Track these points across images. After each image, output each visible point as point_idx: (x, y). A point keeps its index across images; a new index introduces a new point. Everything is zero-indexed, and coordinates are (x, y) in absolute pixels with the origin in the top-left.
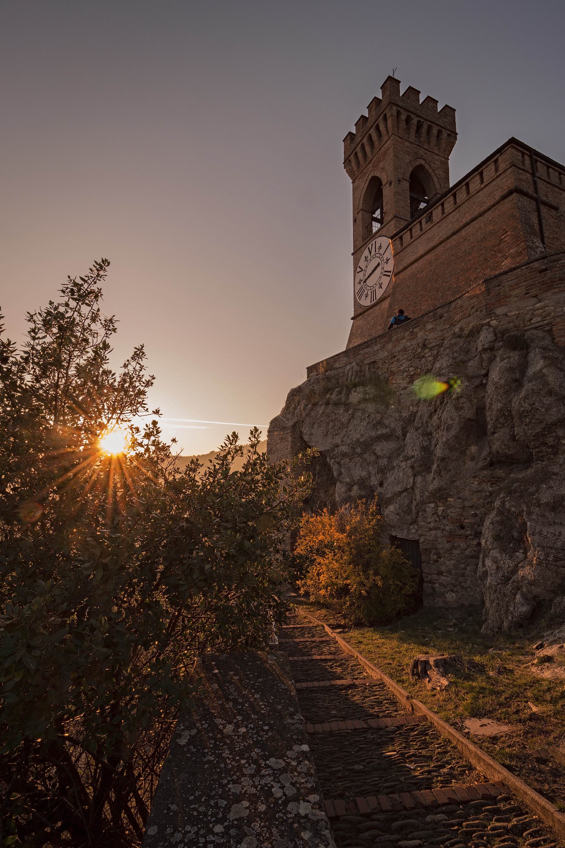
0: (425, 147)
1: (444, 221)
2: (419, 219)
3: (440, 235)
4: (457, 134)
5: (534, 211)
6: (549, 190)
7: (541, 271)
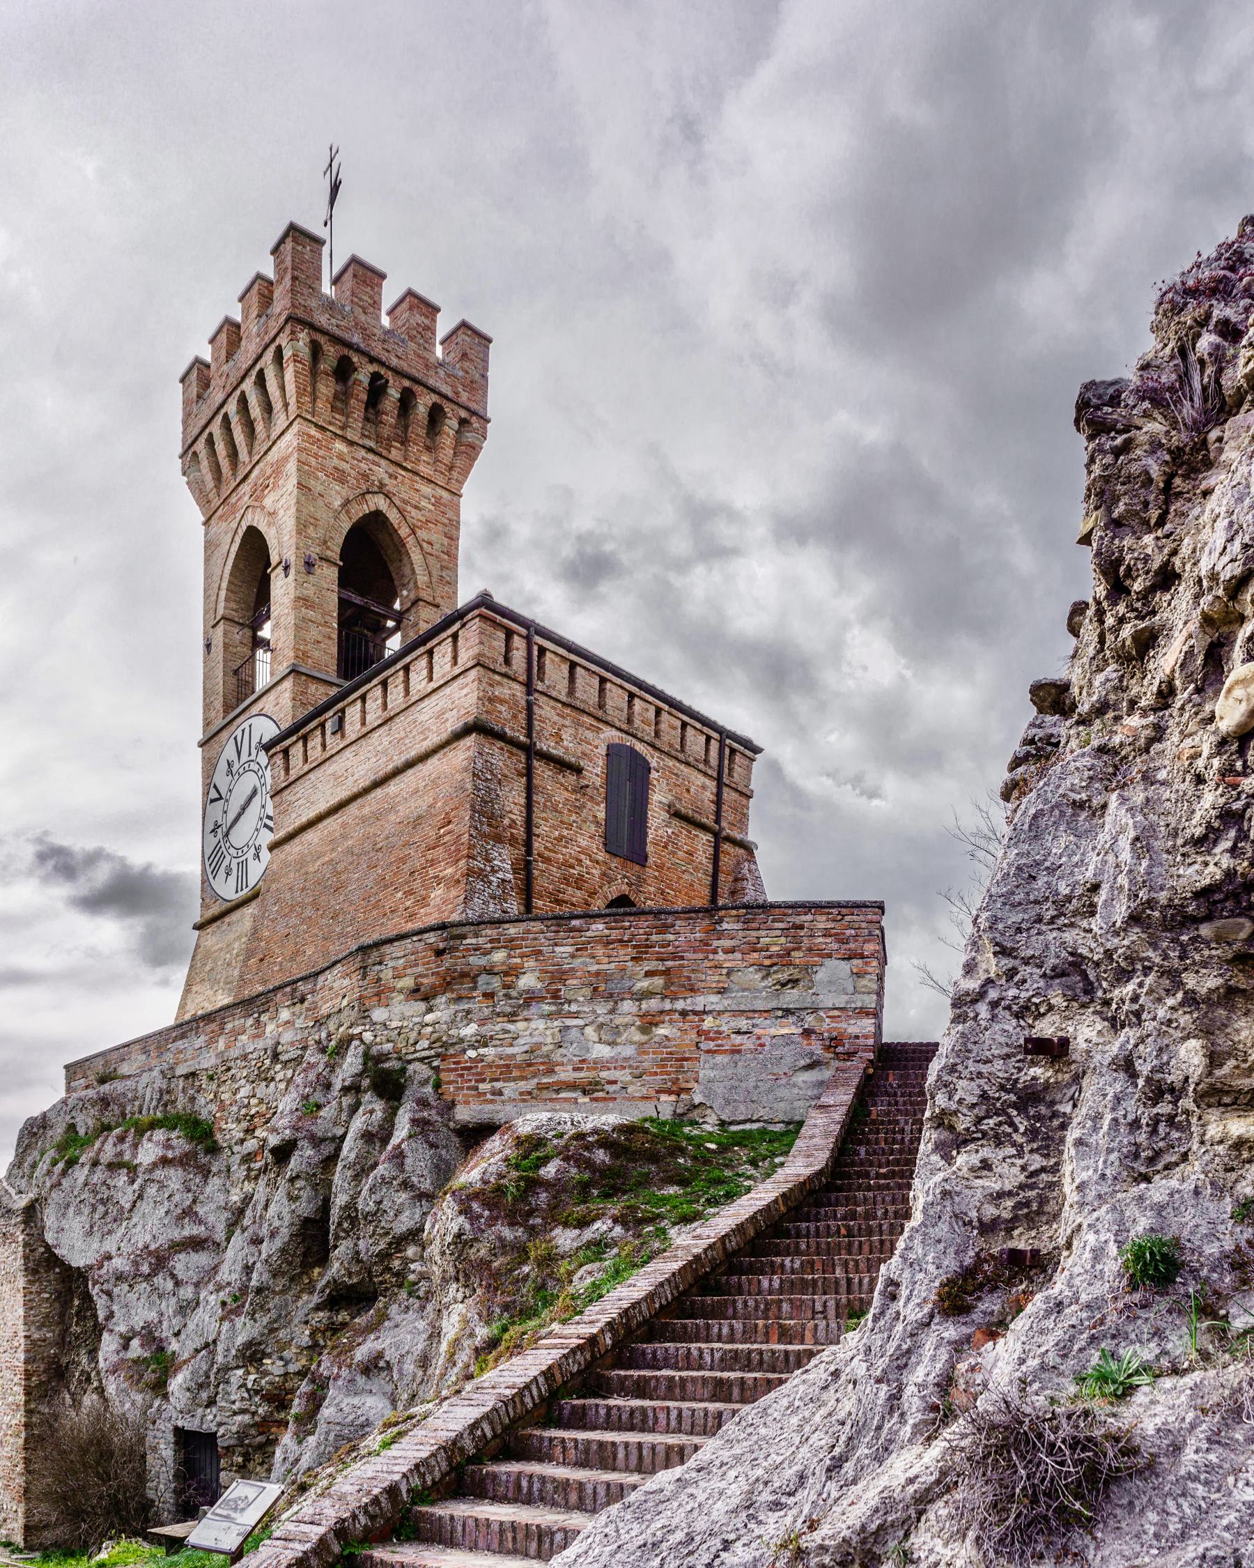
0: (395, 454)
1: (363, 742)
2: (322, 719)
3: (355, 777)
4: (488, 421)
5: (520, 775)
6: (567, 723)
7: (439, 953)
